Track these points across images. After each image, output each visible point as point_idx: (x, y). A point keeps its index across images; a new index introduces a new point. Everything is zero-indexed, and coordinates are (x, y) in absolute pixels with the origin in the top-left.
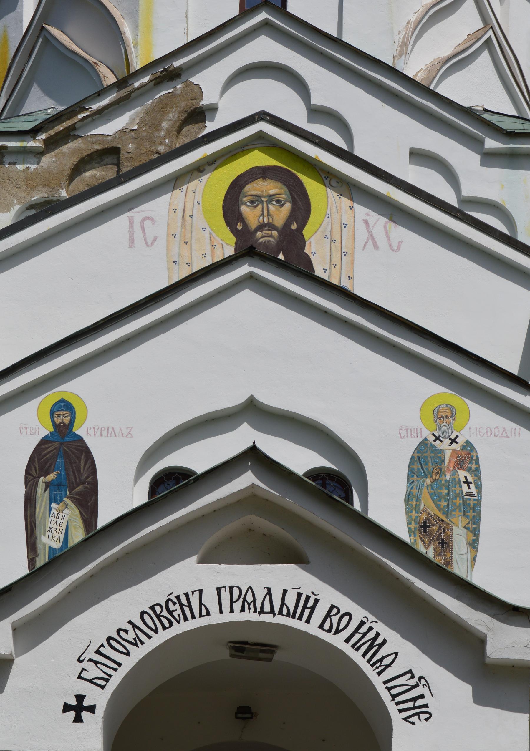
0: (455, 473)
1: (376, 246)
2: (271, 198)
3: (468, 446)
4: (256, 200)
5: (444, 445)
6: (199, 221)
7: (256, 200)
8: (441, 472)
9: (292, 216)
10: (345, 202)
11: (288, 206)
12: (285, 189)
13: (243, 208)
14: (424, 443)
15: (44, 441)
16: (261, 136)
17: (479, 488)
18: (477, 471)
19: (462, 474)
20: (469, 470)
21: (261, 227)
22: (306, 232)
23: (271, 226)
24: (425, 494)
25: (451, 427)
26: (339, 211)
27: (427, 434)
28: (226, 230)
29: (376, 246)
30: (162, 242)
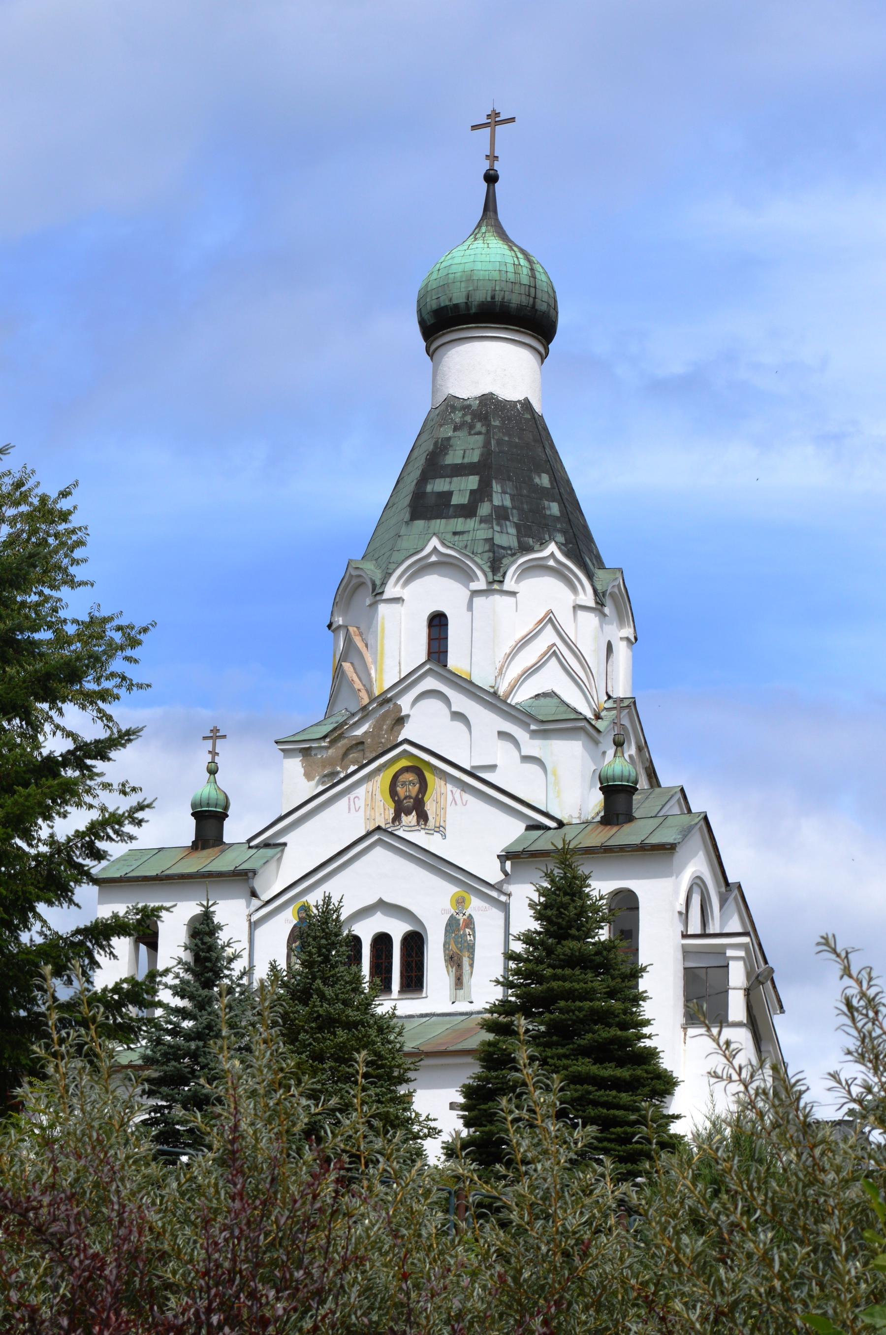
0: (464, 931)
1: (456, 804)
2: (410, 782)
3: (470, 916)
4: (404, 784)
5: (460, 917)
6: (379, 797)
7: (404, 784)
8: (459, 930)
9: (420, 791)
10: (443, 783)
11: (418, 785)
12: (416, 777)
13: (398, 789)
14: (452, 916)
15: (295, 926)
16: (405, 751)
17: (474, 937)
18: (473, 930)
19: (467, 931)
20: (470, 928)
21: (406, 798)
22: (425, 799)
23: (409, 797)
24: (452, 942)
25: (463, 909)
26: (440, 787)
27: (453, 911)
28: (390, 800)
29: (456, 804)
30: (362, 809)
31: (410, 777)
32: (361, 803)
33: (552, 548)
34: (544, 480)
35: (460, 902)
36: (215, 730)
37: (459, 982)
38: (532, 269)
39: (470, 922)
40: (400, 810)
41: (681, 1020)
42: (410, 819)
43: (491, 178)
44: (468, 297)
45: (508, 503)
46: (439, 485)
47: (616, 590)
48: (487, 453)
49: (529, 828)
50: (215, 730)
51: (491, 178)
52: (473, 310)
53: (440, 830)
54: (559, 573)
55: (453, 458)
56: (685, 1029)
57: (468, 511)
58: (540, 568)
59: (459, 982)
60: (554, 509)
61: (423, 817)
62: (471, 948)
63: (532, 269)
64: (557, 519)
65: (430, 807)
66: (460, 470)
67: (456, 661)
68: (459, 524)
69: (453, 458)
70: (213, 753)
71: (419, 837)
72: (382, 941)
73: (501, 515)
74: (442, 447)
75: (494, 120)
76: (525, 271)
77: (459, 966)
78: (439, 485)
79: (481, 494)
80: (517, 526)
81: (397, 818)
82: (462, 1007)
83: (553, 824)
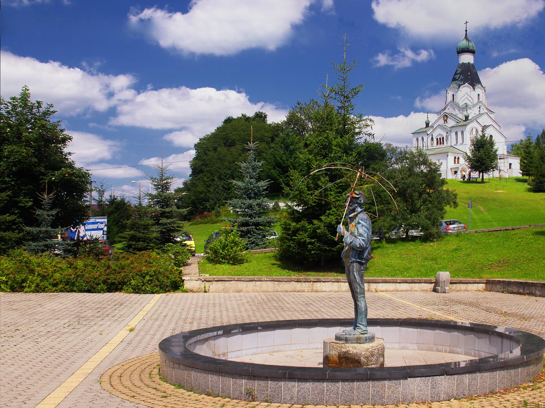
33: (466, 84)
40: (445, 121)
43: (466, 31)
46: (456, 76)
48: (461, 71)
51: (466, 31)
54: (468, 87)
55: (458, 72)
57: (457, 80)
58: (465, 86)
66: (458, 74)
68: (457, 82)
69: (458, 72)
72: (440, 138)
73: (461, 80)
74: (457, 70)
75: (466, 22)
79: (459, 77)
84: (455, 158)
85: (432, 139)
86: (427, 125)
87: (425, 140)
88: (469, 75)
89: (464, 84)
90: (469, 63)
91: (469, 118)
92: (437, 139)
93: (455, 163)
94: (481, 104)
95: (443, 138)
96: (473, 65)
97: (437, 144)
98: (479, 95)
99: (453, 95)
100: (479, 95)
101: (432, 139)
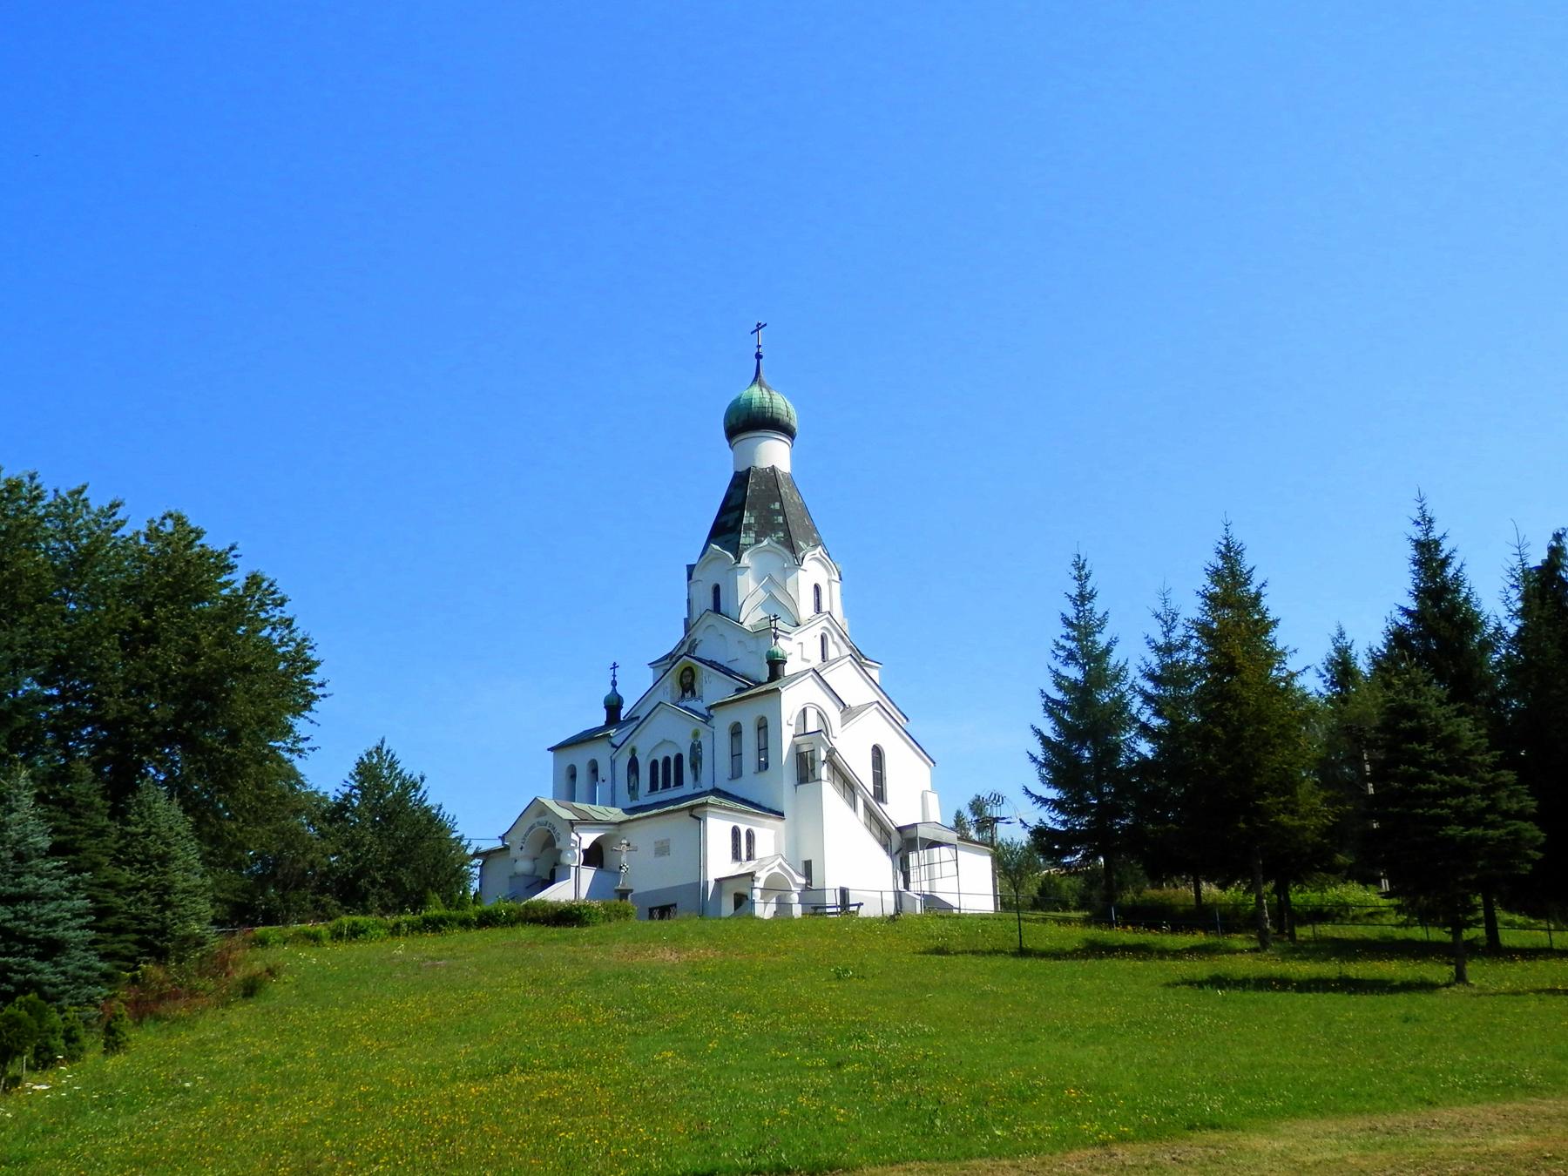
31: (687, 673)
32: (668, 690)
34: (777, 506)
35: (696, 734)
36: (615, 664)
37: (696, 778)
38: (771, 399)
39: (700, 745)
40: (685, 690)
41: (796, 782)
42: (688, 695)
43: (759, 356)
44: (737, 419)
45: (753, 521)
47: (818, 556)
49: (737, 690)
50: (615, 664)
51: (759, 356)
52: (741, 426)
53: (700, 698)
55: (732, 503)
56: (796, 786)
59: (696, 778)
60: (781, 519)
61: (694, 693)
62: (701, 758)
63: (771, 399)
64: (781, 524)
65: (696, 687)
67: (723, 609)
70: (614, 676)
71: (692, 704)
72: (667, 760)
75: (759, 327)
76: (767, 400)
77: (696, 769)
78: (723, 519)
80: (756, 532)
81: (683, 695)
82: (698, 790)
83: (746, 686)
84: (736, 833)
85: (633, 766)
86: (613, 706)
87: (604, 771)
88: (778, 513)
89: (758, 542)
90: (773, 469)
91: (789, 669)
92: (654, 764)
93: (736, 856)
94: (825, 624)
95: (679, 758)
96: (789, 478)
97: (653, 787)
98: (817, 588)
99: (717, 589)
100: (817, 588)
101: (633, 766)
